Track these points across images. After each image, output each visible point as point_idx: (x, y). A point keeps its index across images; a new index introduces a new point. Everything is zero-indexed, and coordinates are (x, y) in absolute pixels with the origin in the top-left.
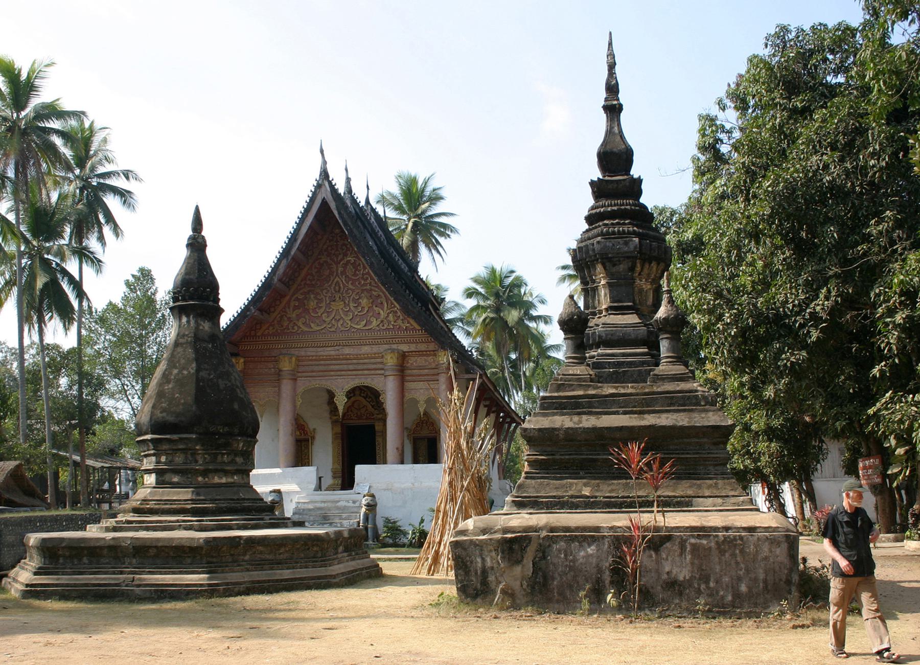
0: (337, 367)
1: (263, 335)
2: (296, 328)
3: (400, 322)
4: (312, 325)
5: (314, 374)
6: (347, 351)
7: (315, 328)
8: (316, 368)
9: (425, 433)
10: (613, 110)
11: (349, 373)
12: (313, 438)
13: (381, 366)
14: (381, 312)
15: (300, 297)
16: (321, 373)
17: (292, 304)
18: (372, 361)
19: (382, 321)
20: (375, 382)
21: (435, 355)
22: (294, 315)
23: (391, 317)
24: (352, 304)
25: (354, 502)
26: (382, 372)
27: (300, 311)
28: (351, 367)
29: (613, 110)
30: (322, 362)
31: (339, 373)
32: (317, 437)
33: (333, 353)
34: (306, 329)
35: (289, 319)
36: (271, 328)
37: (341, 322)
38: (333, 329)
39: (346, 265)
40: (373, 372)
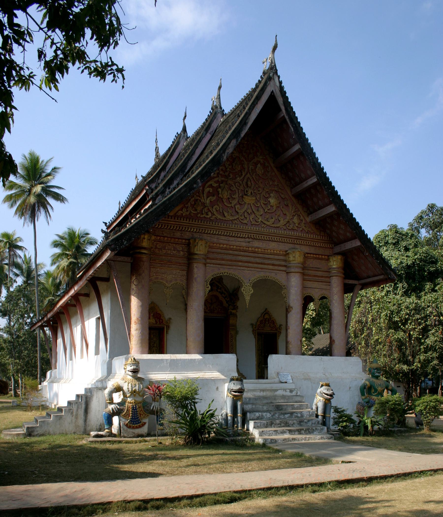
0: (245, 259)
1: (175, 216)
2: (210, 213)
3: (303, 224)
4: (226, 214)
5: (223, 262)
6: (256, 244)
7: (229, 217)
8: (225, 257)
9: (267, 329)
10: (156, 142)
11: (256, 265)
12: (168, 327)
13: (283, 263)
14: (287, 213)
15: (215, 185)
16: (230, 263)
17: (207, 190)
18: (276, 257)
19: (288, 222)
20: (280, 277)
21: (328, 260)
22: (208, 201)
23: (296, 220)
24: (262, 202)
25: (291, 391)
26: (284, 268)
27: (215, 198)
28: (258, 260)
29: (156, 142)
30: (231, 252)
31: (246, 264)
32: (172, 327)
33: (244, 244)
34: (219, 217)
35: (203, 204)
36: (184, 210)
37: (253, 215)
38: (245, 222)
39: (256, 164)
40: (276, 268)
